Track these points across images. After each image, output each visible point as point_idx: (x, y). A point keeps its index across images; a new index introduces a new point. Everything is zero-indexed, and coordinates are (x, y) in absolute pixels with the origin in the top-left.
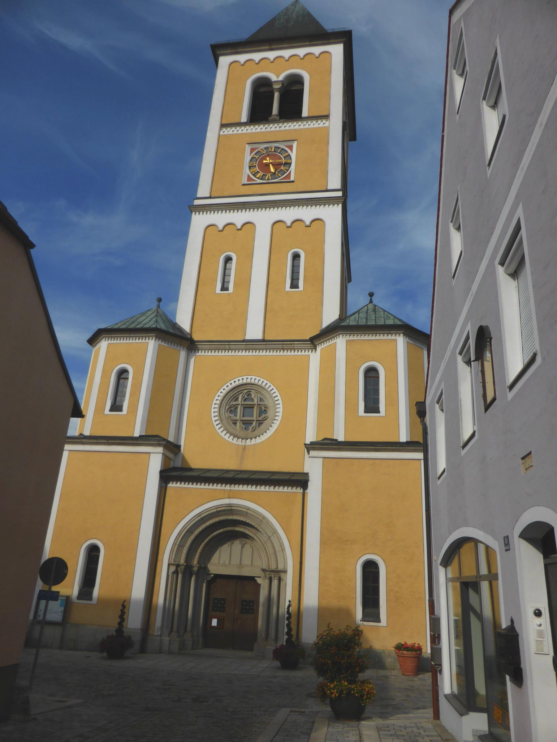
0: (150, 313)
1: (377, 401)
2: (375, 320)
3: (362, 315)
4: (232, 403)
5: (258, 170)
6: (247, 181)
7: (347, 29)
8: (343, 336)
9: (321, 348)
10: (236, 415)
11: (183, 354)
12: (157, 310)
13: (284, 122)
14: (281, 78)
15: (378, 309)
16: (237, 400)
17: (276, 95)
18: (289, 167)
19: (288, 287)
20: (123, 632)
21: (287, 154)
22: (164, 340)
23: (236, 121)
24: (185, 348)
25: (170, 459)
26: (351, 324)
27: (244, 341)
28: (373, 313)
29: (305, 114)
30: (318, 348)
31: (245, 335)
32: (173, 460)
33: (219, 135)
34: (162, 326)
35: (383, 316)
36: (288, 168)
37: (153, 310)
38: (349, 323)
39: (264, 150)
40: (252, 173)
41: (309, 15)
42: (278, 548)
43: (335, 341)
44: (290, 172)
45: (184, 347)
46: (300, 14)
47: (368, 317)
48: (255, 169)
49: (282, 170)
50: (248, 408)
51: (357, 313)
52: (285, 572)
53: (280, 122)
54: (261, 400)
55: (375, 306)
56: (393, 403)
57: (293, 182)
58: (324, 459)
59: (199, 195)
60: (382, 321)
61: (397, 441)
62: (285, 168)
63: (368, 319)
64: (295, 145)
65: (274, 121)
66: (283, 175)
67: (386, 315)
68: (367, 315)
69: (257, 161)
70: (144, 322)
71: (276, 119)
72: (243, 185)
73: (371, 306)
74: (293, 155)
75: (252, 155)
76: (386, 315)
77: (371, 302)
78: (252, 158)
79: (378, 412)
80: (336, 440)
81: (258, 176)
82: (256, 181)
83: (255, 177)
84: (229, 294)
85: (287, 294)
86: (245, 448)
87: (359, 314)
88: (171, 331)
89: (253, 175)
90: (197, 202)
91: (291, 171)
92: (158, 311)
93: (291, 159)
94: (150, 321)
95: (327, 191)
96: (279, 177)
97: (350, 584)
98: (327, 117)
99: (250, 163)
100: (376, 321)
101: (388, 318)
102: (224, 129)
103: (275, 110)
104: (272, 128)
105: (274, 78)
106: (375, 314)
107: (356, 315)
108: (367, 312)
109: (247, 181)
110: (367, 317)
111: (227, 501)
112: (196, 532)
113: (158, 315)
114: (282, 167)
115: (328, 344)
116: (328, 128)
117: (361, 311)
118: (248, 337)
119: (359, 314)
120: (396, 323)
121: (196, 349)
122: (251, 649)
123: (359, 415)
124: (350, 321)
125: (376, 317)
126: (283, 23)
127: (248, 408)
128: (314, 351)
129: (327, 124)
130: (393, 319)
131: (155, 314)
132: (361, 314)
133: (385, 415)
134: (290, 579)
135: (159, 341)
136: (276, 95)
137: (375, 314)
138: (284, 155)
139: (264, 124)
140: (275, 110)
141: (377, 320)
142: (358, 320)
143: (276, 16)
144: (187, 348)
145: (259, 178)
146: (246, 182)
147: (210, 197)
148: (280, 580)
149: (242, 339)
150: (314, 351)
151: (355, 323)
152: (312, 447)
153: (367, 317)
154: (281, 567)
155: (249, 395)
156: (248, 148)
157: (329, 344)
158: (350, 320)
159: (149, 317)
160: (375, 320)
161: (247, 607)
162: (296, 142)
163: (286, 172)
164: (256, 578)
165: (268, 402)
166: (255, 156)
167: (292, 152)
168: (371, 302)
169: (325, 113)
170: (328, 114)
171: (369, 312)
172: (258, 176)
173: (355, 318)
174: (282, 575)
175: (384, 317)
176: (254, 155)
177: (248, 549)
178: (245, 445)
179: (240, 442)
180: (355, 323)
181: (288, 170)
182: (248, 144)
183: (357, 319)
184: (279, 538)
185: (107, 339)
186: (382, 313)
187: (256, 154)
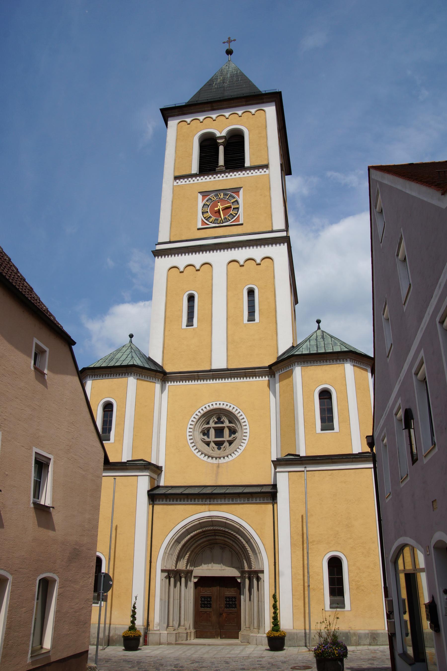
0: (125, 349)
1: (331, 419)
2: (325, 347)
3: (313, 342)
4: (204, 427)
5: (210, 215)
6: (202, 226)
7: (277, 91)
8: (298, 363)
9: (280, 374)
10: (208, 437)
11: (158, 386)
12: (130, 345)
13: (229, 173)
14: (224, 134)
15: (326, 336)
16: (208, 423)
17: (221, 149)
18: (238, 211)
19: (245, 321)
21: (235, 200)
22: (141, 374)
23: (187, 173)
24: (159, 380)
25: (155, 479)
26: (304, 353)
27: (211, 371)
28: (322, 340)
29: (247, 164)
30: (277, 373)
31: (211, 364)
32: (156, 480)
33: (173, 185)
34: (138, 362)
35: (331, 343)
36: (236, 212)
37: (126, 346)
38: (302, 352)
39: (214, 197)
40: (205, 218)
41: (242, 75)
43: (291, 368)
44: (239, 215)
45: (158, 379)
46: (234, 74)
47: (318, 344)
48: (208, 215)
49: (231, 214)
51: (308, 341)
52: (262, 572)
53: (227, 173)
55: (323, 332)
56: (346, 421)
57: (242, 224)
58: (290, 473)
60: (330, 347)
61: (351, 453)
62: (234, 212)
63: (318, 346)
65: (221, 172)
66: (233, 218)
67: (334, 341)
68: (317, 342)
69: (208, 207)
70: (122, 359)
71: (222, 169)
72: (198, 229)
73: (319, 332)
74: (240, 200)
75: (204, 202)
76: (334, 341)
77: (319, 328)
78: (204, 205)
79: (333, 429)
80: (299, 455)
81: (211, 220)
82: (209, 225)
83: (208, 221)
84: (194, 329)
85: (245, 326)
86: (218, 466)
87: (310, 342)
88: (147, 366)
89: (206, 220)
91: (239, 215)
92: (131, 347)
93: (238, 204)
94: (127, 357)
95: (272, 232)
96: (230, 220)
97: (318, 578)
98: (266, 166)
99: (202, 209)
100: (325, 349)
101: (336, 344)
102: (178, 181)
103: (221, 162)
104: (220, 177)
105: (218, 134)
106: (324, 341)
107: (308, 343)
108: (316, 339)
109: (202, 226)
110: (317, 344)
112: (183, 542)
113: (132, 351)
114: (231, 211)
115: (285, 371)
117: (311, 338)
118: (214, 367)
119: (310, 342)
120: (342, 350)
121: (168, 380)
122: (237, 638)
123: (317, 432)
124: (303, 349)
125: (324, 344)
126: (220, 83)
128: (273, 376)
129: (267, 172)
130: (340, 346)
131: (129, 351)
132: (311, 342)
133: (339, 431)
134: (267, 577)
135: (137, 376)
136: (221, 149)
137: (324, 341)
138: (232, 201)
139: (212, 175)
140: (221, 162)
141: (326, 347)
142: (310, 348)
143: (213, 77)
144: (161, 380)
145: (211, 222)
146: (200, 226)
147: (170, 242)
148: (258, 579)
149: (209, 369)
150: (273, 376)
151: (307, 351)
152: (278, 463)
153: (317, 344)
156: (200, 197)
157: (286, 370)
158: (302, 348)
159: (125, 354)
160: (325, 347)
161: (231, 603)
162: (242, 189)
163: (235, 216)
164: (236, 578)
166: (207, 203)
167: (239, 197)
168: (319, 328)
169: (265, 163)
170: (267, 163)
171: (318, 339)
172: (211, 220)
173: (307, 346)
174: (260, 575)
175: (332, 344)
176: (205, 202)
178: (219, 464)
179: (214, 461)
180: (307, 351)
181: (236, 214)
182: (199, 192)
183: (309, 347)
185: (91, 376)
186: (330, 339)
187: (207, 201)
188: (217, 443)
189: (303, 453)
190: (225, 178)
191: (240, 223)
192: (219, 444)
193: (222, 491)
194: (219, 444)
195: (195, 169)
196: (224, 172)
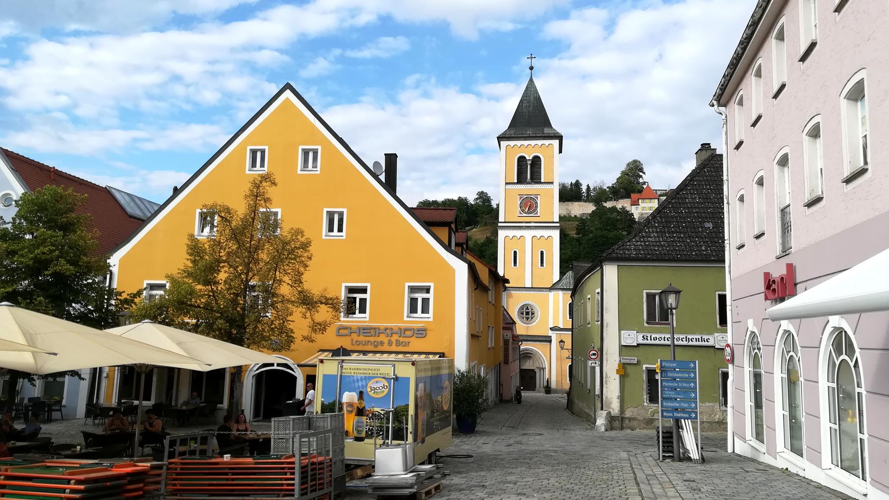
14: (531, 158)
16: (523, 309)
17: (529, 166)
20: (550, 388)
29: (542, 181)
42: (543, 361)
50: (527, 313)
54: (532, 309)
59: (500, 221)
64: (539, 196)
74: (538, 202)
90: (499, 224)
95: (553, 222)
98: (552, 183)
102: (507, 185)
103: (529, 177)
105: (528, 158)
111: (525, 347)
116: (553, 189)
118: (526, 286)
127: (527, 313)
134: (547, 370)
136: (529, 166)
139: (525, 184)
147: (505, 222)
154: (544, 367)
155: (528, 308)
165: (534, 310)
177: (531, 361)
184: (543, 359)
188: (526, 318)
189: (562, 327)
190: (531, 187)
191: (538, 215)
192: (528, 318)
193: (531, 339)
194: (528, 318)
195: (516, 181)
196: (530, 183)
